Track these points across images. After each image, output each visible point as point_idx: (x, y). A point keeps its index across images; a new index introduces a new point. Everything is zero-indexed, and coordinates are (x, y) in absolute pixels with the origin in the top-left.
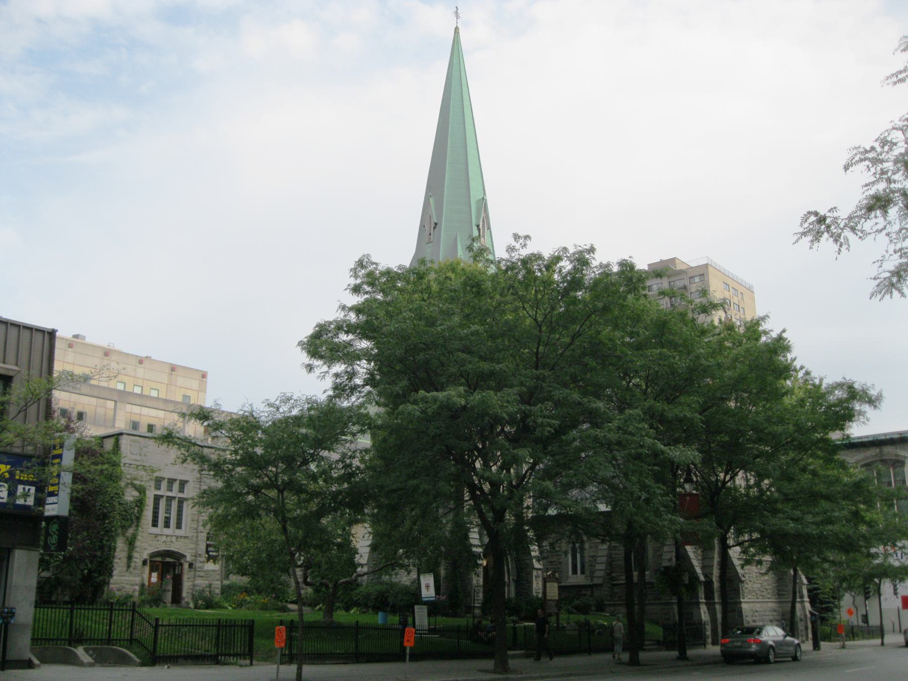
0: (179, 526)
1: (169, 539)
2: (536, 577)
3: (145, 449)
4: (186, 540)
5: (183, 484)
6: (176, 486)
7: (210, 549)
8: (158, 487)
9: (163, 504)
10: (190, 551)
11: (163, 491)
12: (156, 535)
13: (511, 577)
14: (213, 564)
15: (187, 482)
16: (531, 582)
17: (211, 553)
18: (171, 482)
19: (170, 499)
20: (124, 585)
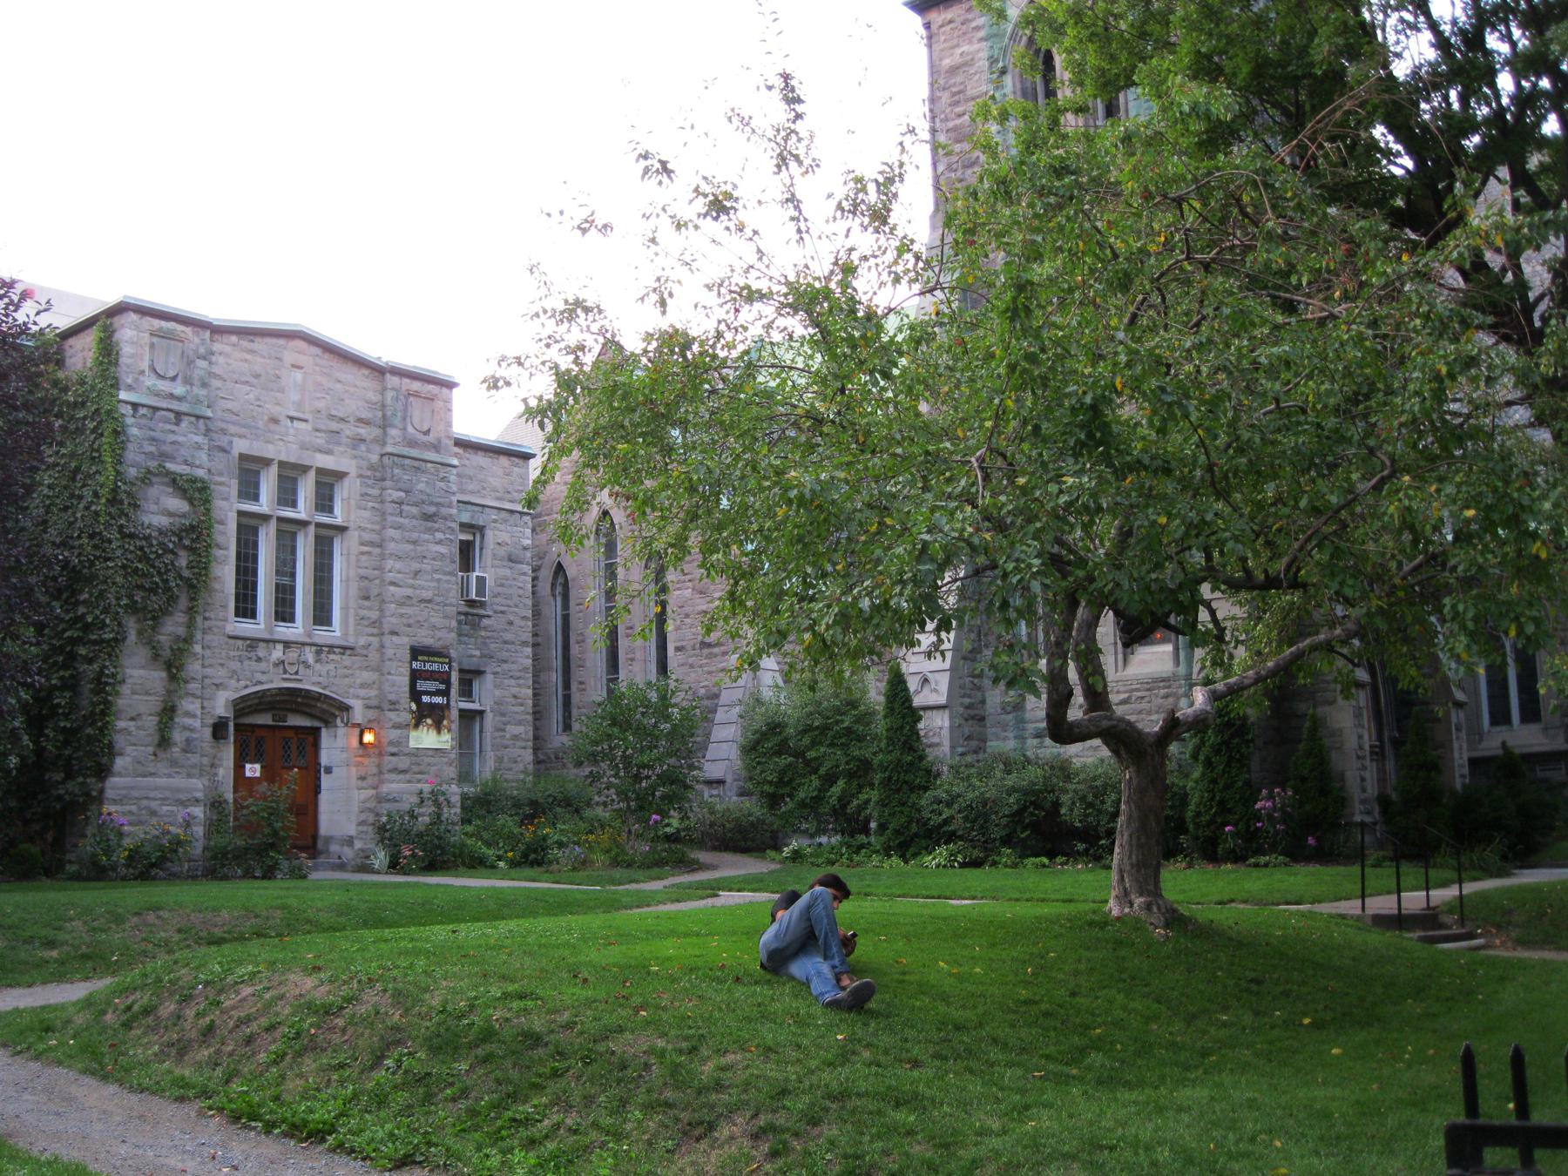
0: (322, 615)
1: (293, 655)
3: (202, 364)
4: (347, 660)
5: (327, 483)
6: (306, 490)
7: (422, 685)
8: (250, 490)
10: (362, 692)
12: (253, 643)
13: (1386, 734)
14: (433, 733)
15: (340, 476)
17: (426, 699)
18: (290, 476)
20: (154, 805)
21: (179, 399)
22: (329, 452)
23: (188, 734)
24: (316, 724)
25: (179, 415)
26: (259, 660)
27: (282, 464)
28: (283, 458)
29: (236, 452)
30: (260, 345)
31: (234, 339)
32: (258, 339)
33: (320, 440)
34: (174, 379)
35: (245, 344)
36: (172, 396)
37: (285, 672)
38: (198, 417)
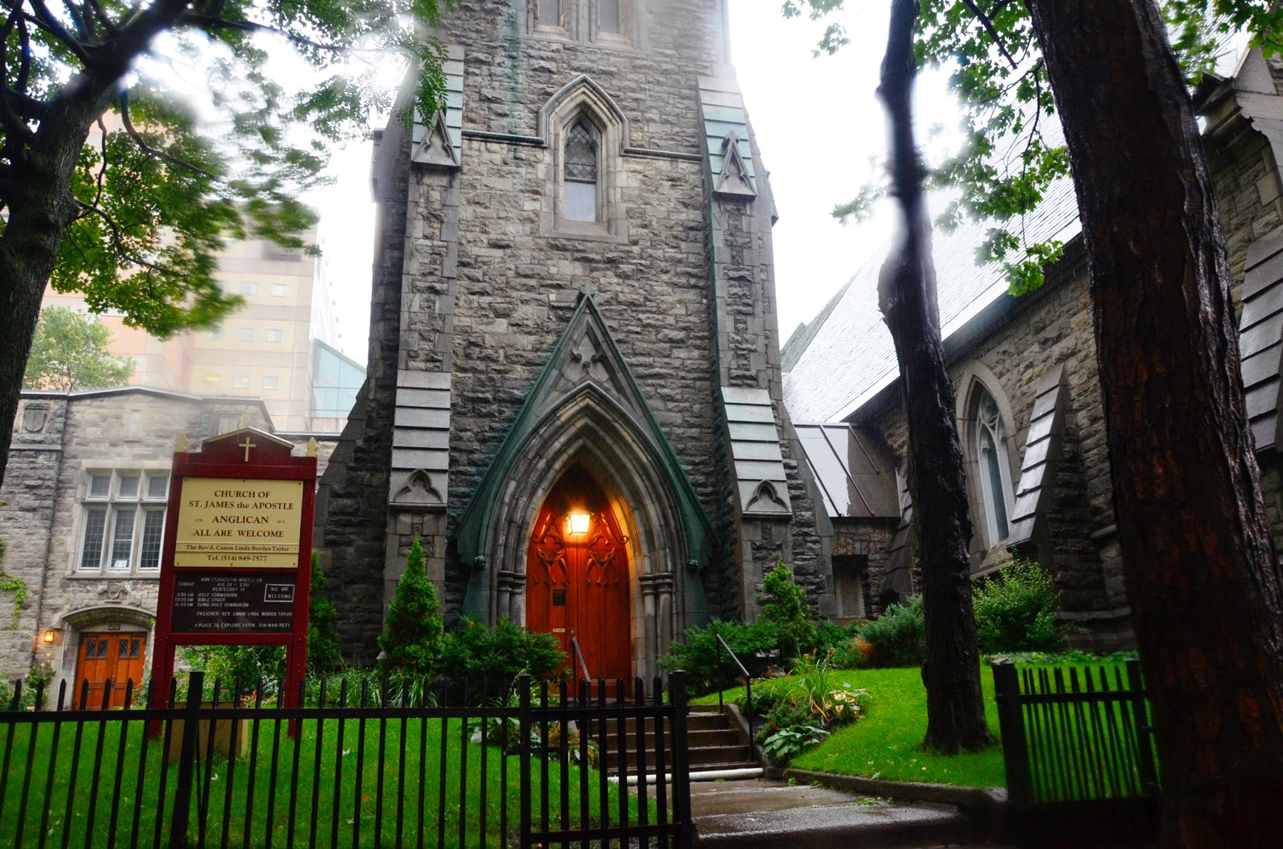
2: (757, 548)
9: (110, 520)
11: (113, 493)
16: (739, 571)
19: (125, 512)
21: (40, 442)
22: (154, 457)
23: (24, 640)
24: (142, 630)
25: (37, 451)
26: (88, 591)
27: (120, 472)
28: (119, 466)
29: (83, 468)
30: (107, 402)
31: (88, 402)
32: (106, 399)
33: (148, 451)
34: (39, 431)
35: (96, 403)
36: (34, 442)
37: (109, 598)
38: (50, 451)
